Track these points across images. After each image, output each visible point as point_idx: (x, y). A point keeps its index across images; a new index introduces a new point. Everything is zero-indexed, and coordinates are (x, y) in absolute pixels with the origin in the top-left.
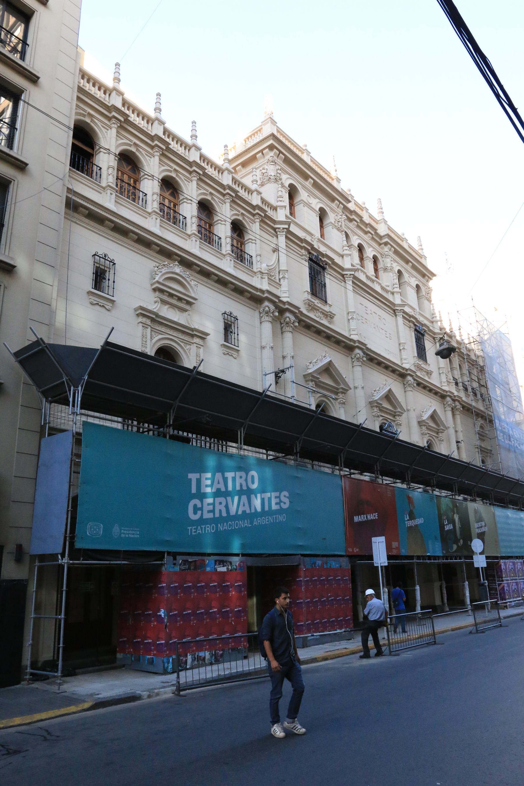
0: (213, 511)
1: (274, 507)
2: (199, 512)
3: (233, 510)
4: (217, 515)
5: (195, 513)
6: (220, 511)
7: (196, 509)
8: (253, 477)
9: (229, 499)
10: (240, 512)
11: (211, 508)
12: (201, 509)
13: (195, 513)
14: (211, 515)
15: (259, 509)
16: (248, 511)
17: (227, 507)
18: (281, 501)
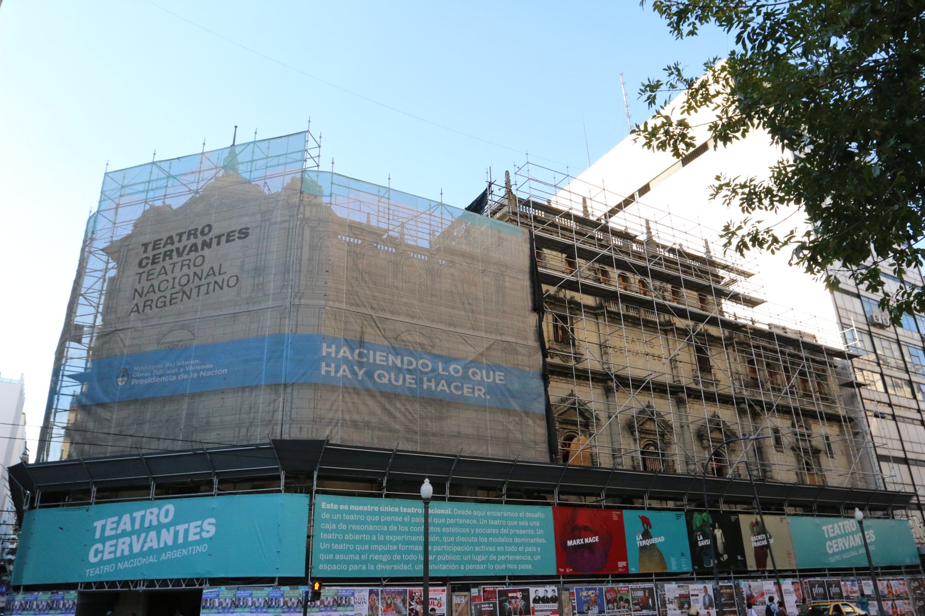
0: (115, 552)
1: (191, 538)
2: (100, 555)
3: (136, 549)
4: (119, 554)
5: (96, 556)
6: (123, 550)
7: (97, 552)
8: (167, 511)
9: (134, 537)
10: (145, 549)
11: (113, 549)
12: (102, 552)
13: (96, 556)
14: (112, 556)
15: (170, 543)
16: (155, 546)
17: (131, 546)
18: (202, 530)
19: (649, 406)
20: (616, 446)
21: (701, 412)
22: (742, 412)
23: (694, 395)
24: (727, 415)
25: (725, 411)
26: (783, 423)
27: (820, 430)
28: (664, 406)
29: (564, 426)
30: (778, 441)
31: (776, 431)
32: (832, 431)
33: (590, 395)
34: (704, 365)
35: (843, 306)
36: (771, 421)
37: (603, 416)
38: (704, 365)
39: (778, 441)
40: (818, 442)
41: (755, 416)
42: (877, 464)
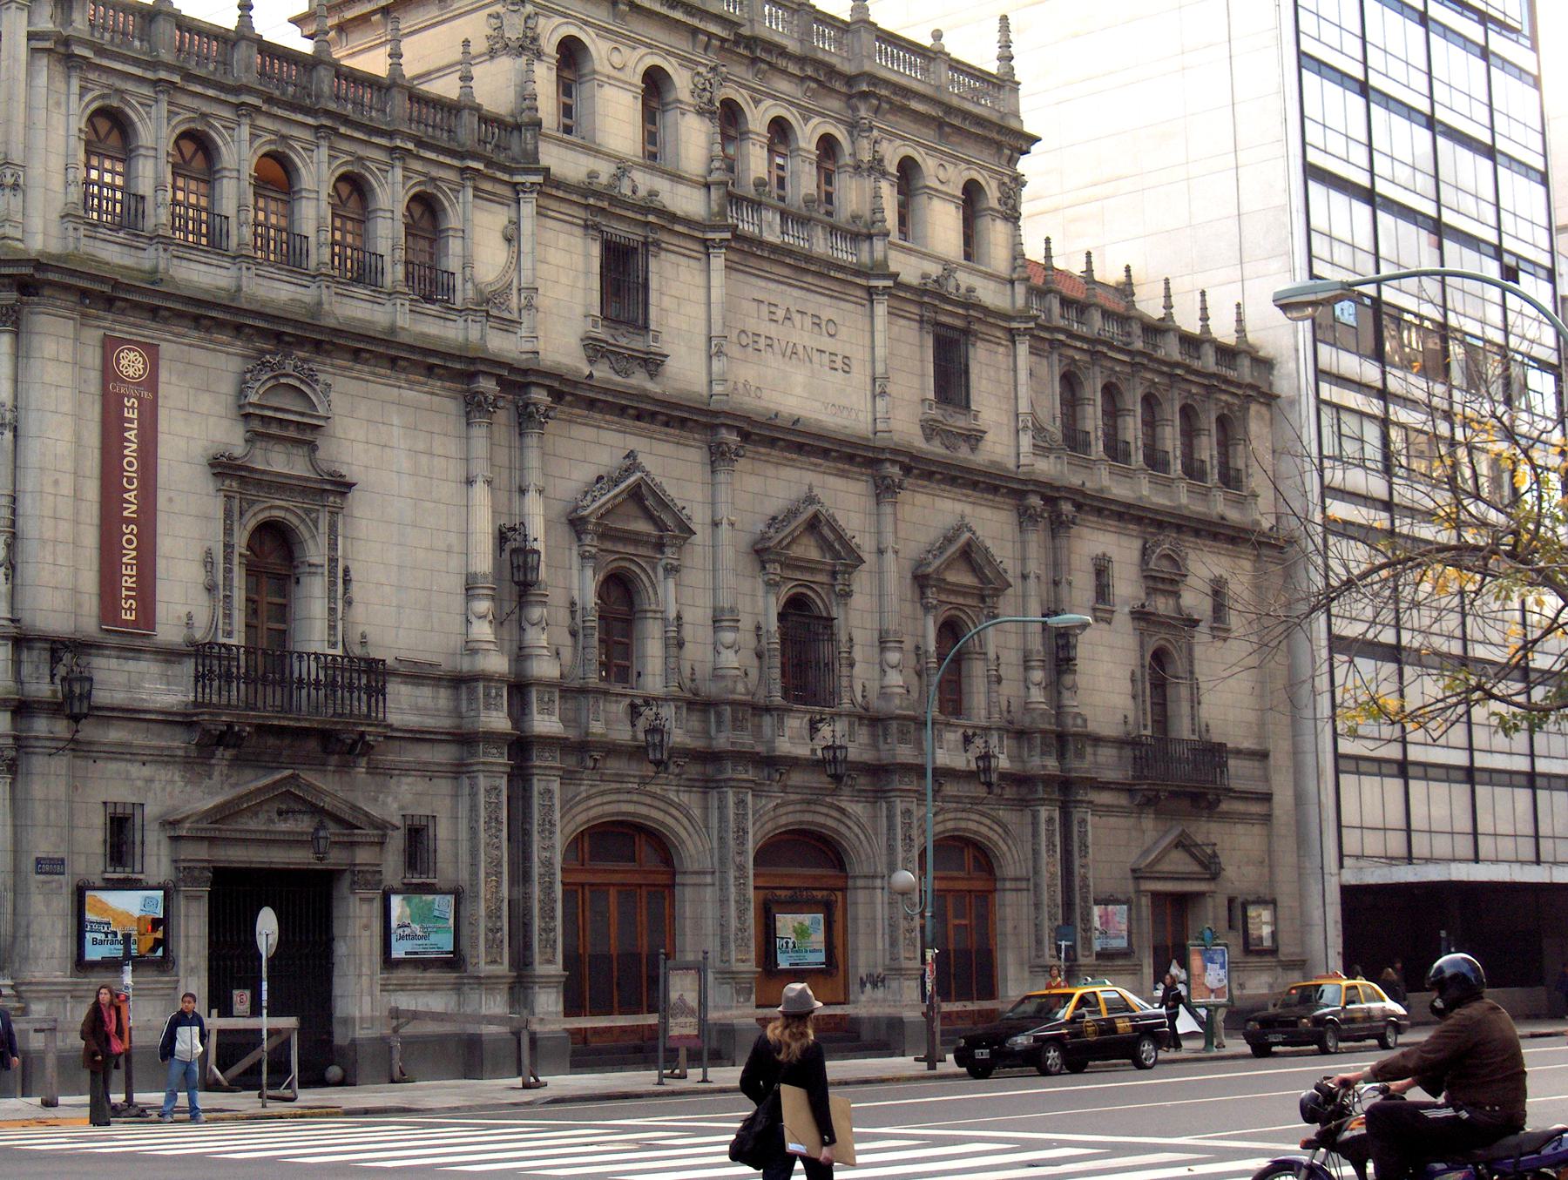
19: (810, 499)
20: (725, 601)
21: (930, 514)
22: (1025, 517)
23: (920, 469)
24: (992, 525)
25: (987, 513)
26: (1121, 549)
27: (1205, 565)
28: (846, 499)
29: (609, 545)
30: (1102, 591)
31: (1101, 569)
32: (1237, 572)
33: (674, 468)
34: (951, 381)
35: (1324, 227)
36: (1095, 541)
37: (699, 517)
38: (951, 381)
39: (1102, 591)
40: (1194, 600)
41: (1058, 526)
42: (1324, 653)
